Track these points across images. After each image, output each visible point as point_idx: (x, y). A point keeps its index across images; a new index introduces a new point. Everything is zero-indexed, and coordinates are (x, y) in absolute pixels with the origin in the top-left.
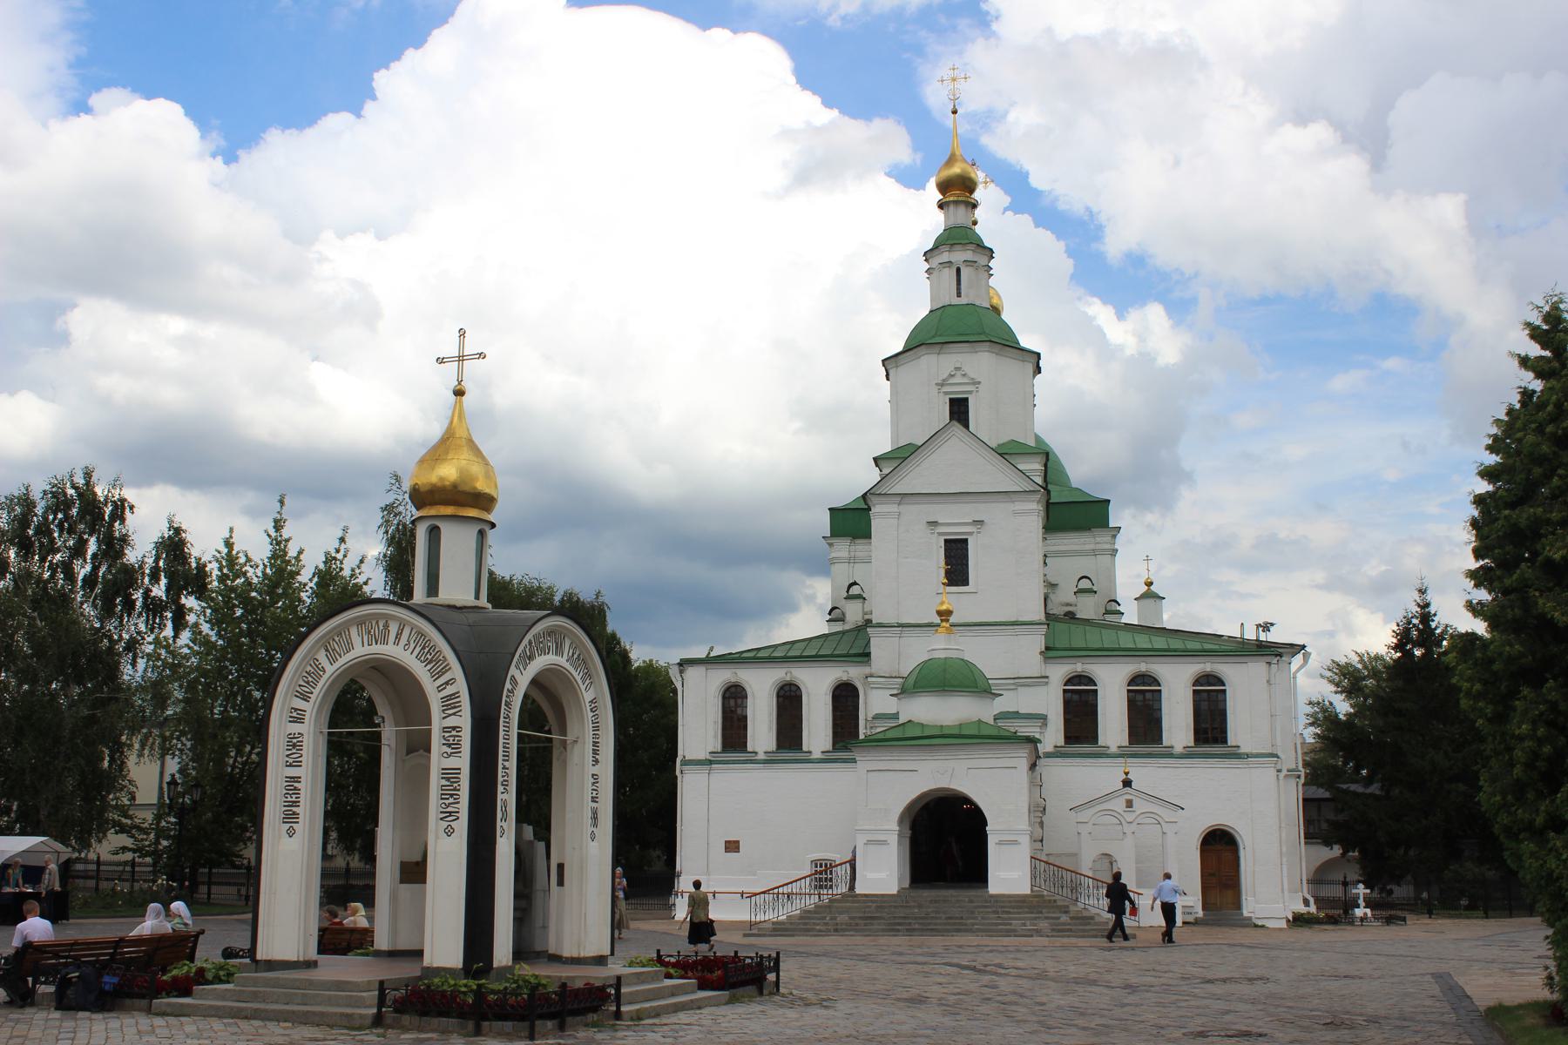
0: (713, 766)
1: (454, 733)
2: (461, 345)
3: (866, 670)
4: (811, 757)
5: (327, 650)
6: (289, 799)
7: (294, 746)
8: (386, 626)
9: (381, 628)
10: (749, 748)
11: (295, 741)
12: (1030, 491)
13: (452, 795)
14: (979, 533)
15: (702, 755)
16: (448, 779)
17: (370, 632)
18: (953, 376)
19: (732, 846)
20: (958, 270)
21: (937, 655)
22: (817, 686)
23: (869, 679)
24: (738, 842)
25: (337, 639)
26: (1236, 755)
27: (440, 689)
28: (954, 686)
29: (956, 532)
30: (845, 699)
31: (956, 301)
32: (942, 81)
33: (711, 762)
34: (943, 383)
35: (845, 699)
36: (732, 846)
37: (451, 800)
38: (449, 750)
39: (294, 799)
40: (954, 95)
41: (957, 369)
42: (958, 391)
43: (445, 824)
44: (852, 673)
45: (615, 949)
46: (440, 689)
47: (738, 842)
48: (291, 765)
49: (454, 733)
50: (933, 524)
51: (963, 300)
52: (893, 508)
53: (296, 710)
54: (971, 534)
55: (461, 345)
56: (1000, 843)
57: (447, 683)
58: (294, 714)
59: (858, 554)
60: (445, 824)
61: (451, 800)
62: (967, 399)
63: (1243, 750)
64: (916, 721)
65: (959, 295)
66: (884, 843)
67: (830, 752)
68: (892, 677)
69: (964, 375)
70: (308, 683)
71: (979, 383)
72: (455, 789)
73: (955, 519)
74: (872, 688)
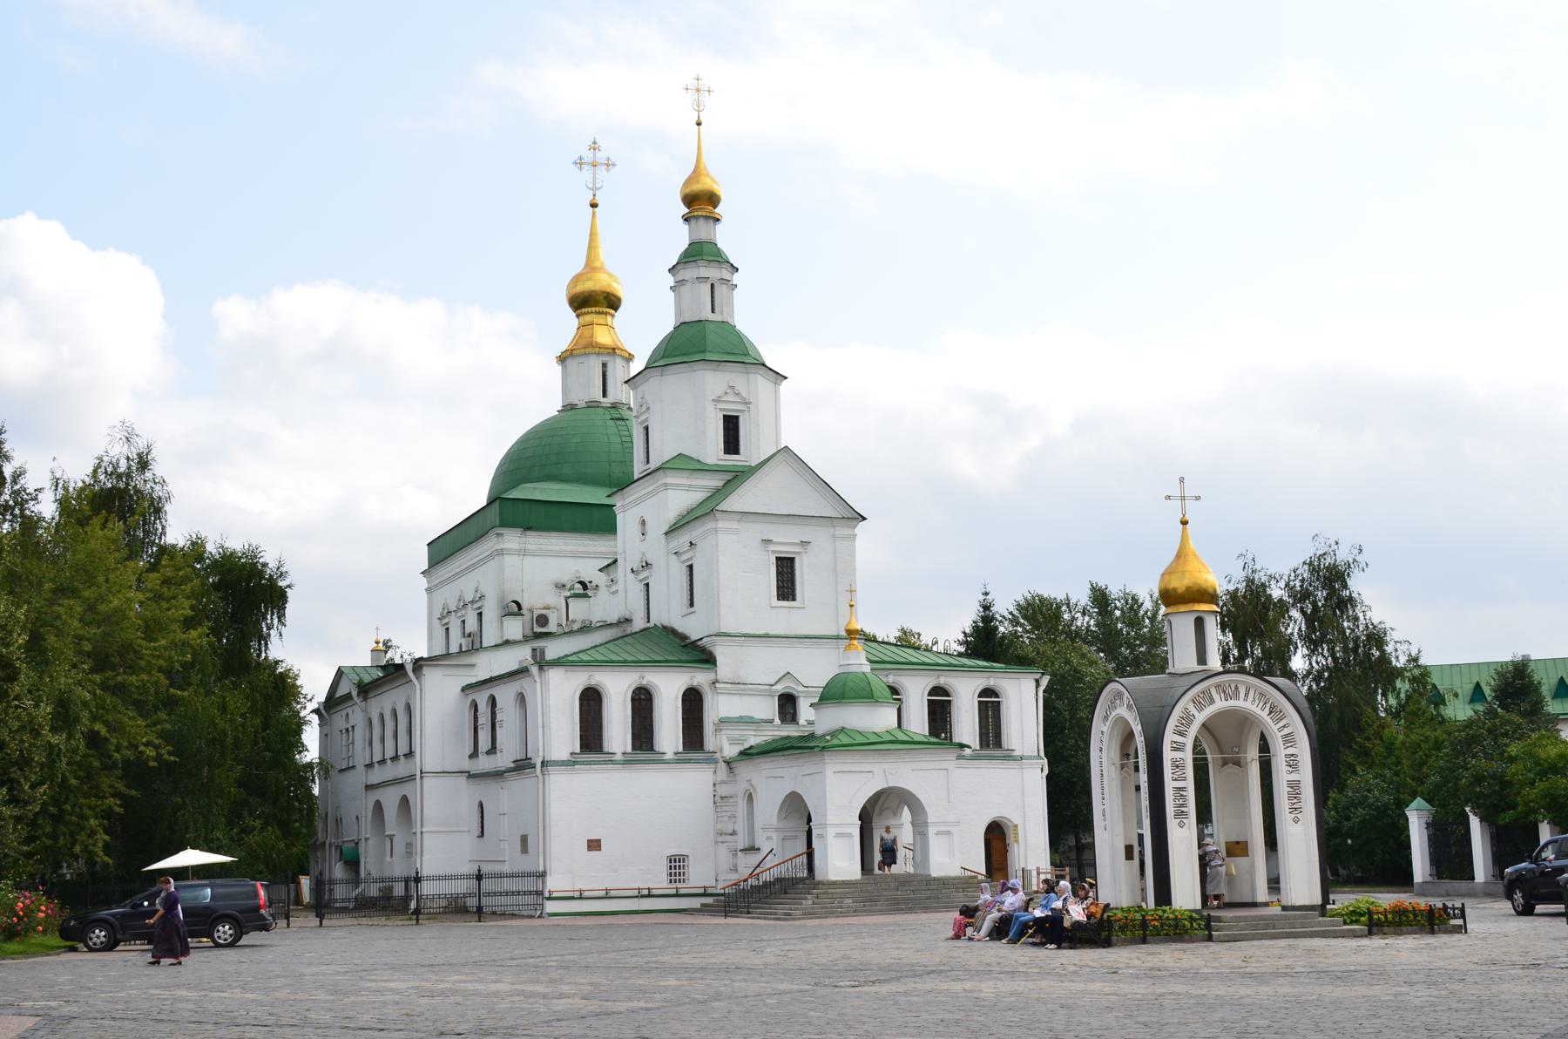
0: (576, 766)
1: (1292, 758)
2: (1182, 489)
3: (710, 676)
4: (665, 758)
5: (1194, 703)
6: (1178, 802)
7: (1177, 766)
8: (1237, 688)
9: (1233, 689)
10: (606, 749)
11: (1177, 763)
12: (848, 518)
13: (1295, 798)
14: (806, 553)
15: (563, 755)
16: (1292, 787)
17: (1225, 692)
18: (726, 393)
19: (594, 845)
20: (712, 285)
21: (852, 669)
22: (669, 687)
23: (717, 685)
24: (600, 840)
25: (1201, 696)
26: (1009, 757)
27: (1280, 730)
28: (851, 698)
29: (786, 551)
30: (693, 702)
31: (711, 317)
32: (687, 89)
33: (575, 763)
34: (717, 400)
35: (693, 702)
36: (594, 845)
37: (1295, 801)
38: (1291, 769)
39: (1181, 802)
40: (698, 106)
41: (733, 388)
42: (732, 409)
43: (1293, 816)
44: (700, 678)
45: (1239, 901)
46: (1280, 730)
47: (600, 840)
48: (1176, 780)
49: (1292, 758)
50: (767, 541)
51: (716, 317)
52: (734, 525)
53: (1175, 742)
54: (799, 553)
55: (1182, 489)
56: (938, 833)
57: (1284, 726)
58: (1174, 745)
59: (528, 546)
60: (1293, 816)
61: (1295, 801)
62: (737, 417)
63: (1015, 753)
64: (849, 728)
65: (713, 311)
66: (850, 835)
67: (680, 753)
68: (735, 684)
69: (737, 394)
70: (1182, 724)
71: (750, 403)
72: (1297, 794)
73: (786, 539)
74: (718, 693)
